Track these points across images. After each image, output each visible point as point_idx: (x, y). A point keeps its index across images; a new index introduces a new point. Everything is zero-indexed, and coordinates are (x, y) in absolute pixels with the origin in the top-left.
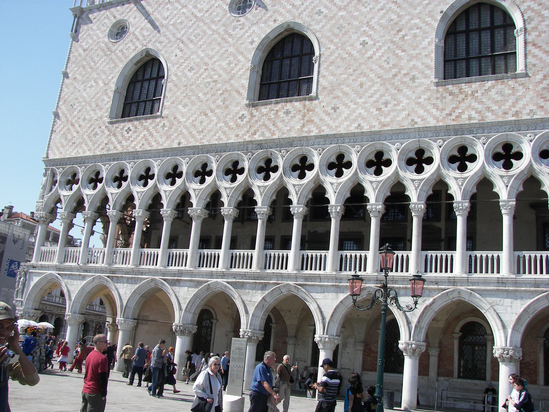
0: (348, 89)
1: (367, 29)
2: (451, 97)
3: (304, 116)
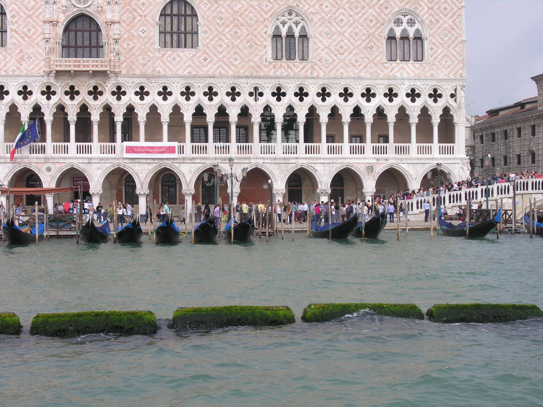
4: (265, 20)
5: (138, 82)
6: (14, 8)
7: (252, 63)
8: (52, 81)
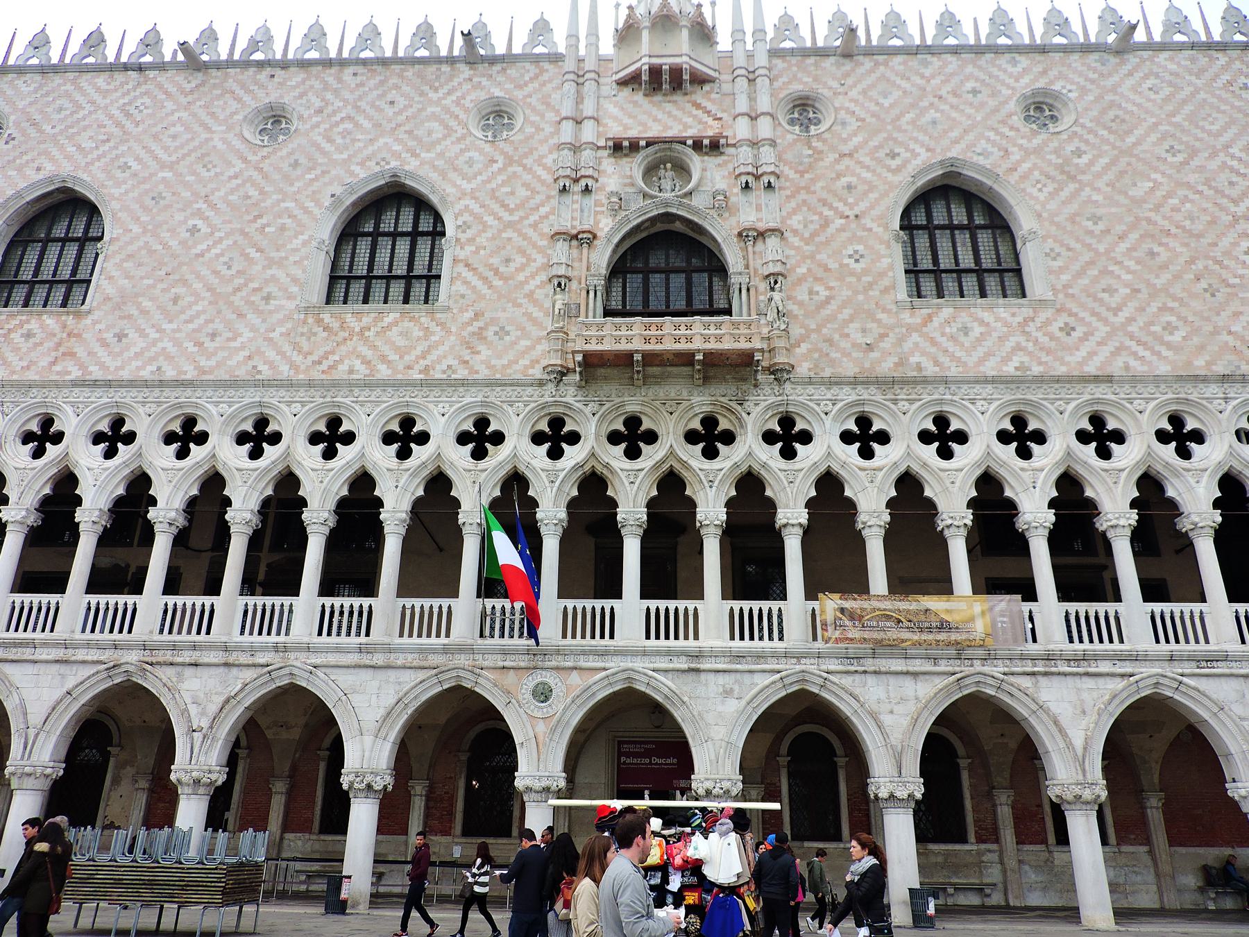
0: (150, 304)
1: (205, 206)
2: (325, 334)
3: (59, 344)
4: (1236, 219)
5: (851, 399)
6: (467, 207)
8: (569, 399)
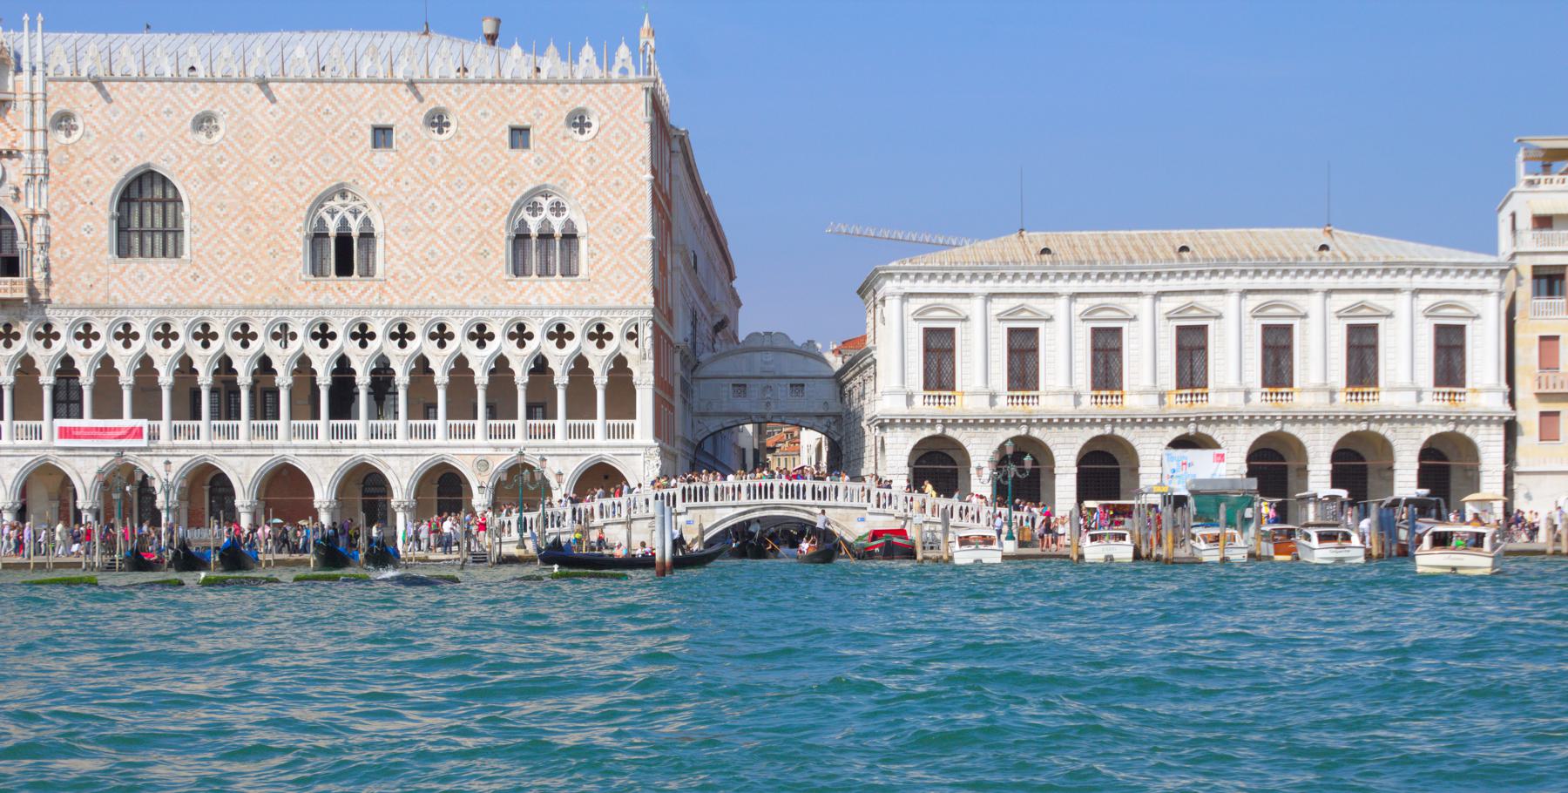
7: (275, 283)
